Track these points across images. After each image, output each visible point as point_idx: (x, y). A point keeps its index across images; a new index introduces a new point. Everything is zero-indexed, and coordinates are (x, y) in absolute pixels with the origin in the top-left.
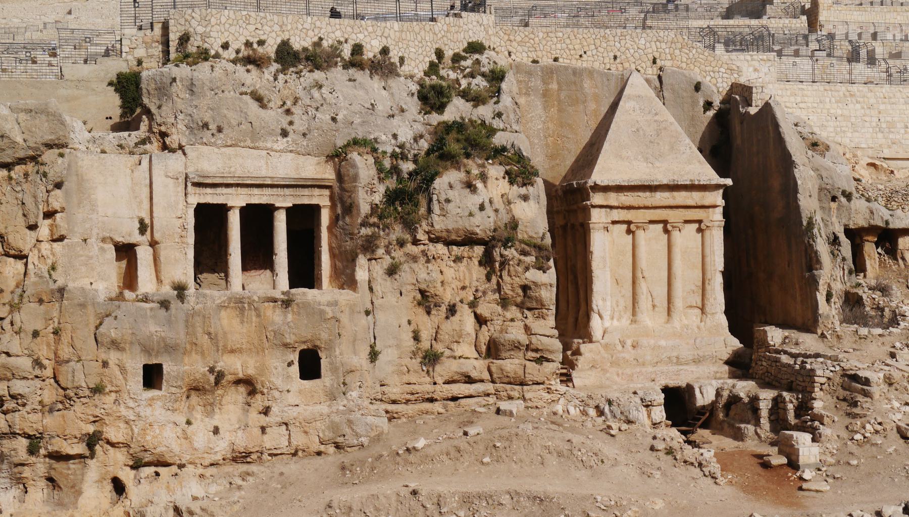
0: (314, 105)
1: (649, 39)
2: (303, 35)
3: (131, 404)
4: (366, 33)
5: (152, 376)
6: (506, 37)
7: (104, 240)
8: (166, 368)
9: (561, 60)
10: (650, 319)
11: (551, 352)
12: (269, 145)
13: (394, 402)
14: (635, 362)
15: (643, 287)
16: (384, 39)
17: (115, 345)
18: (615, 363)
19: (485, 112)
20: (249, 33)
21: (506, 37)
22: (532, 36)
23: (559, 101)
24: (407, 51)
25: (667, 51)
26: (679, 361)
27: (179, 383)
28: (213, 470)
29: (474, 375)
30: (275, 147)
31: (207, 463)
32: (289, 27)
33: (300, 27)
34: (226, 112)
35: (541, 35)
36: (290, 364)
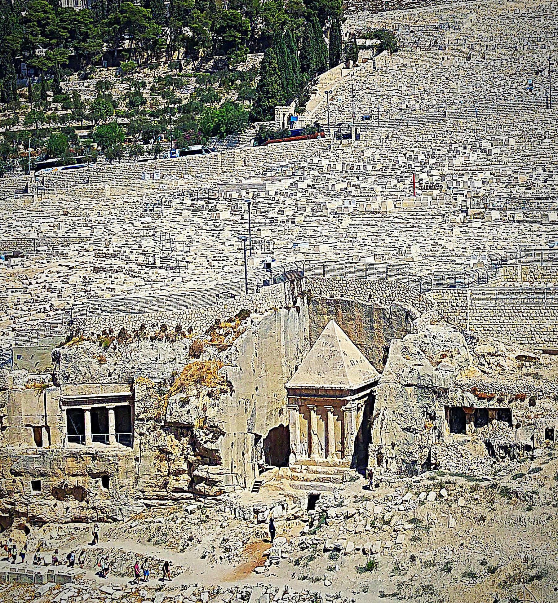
0: (127, 360)
1: (387, 285)
2: (134, 324)
3: (26, 497)
4: (169, 318)
5: (36, 486)
6: (320, 283)
7: (27, 426)
8: (42, 482)
9: (345, 296)
10: (317, 456)
11: (217, 482)
12: (101, 382)
13: (150, 499)
14: (302, 479)
15: (315, 438)
16: (179, 320)
17: (17, 474)
18: (293, 479)
19: (223, 354)
20: (106, 326)
21: (320, 283)
22: (331, 282)
23: (342, 319)
24: (195, 323)
25: (396, 292)
26: (323, 480)
27: (49, 489)
28: (66, 525)
29: (186, 488)
30: (105, 382)
31: (63, 522)
32: (127, 321)
33: (132, 320)
34: (80, 368)
35: (335, 282)
36: (97, 482)
